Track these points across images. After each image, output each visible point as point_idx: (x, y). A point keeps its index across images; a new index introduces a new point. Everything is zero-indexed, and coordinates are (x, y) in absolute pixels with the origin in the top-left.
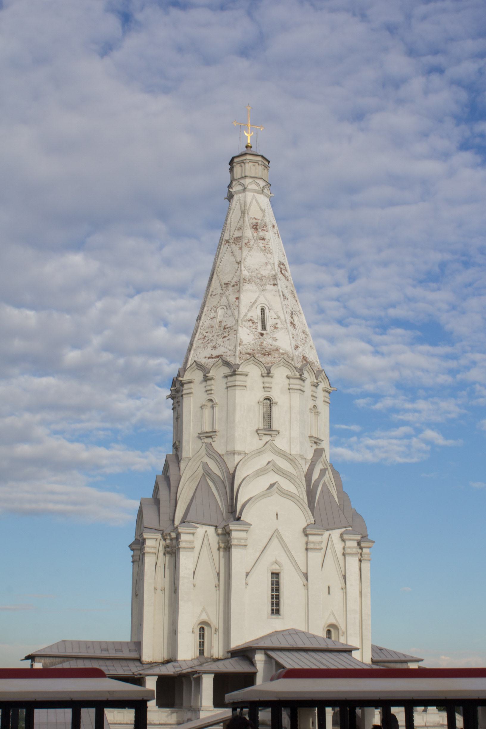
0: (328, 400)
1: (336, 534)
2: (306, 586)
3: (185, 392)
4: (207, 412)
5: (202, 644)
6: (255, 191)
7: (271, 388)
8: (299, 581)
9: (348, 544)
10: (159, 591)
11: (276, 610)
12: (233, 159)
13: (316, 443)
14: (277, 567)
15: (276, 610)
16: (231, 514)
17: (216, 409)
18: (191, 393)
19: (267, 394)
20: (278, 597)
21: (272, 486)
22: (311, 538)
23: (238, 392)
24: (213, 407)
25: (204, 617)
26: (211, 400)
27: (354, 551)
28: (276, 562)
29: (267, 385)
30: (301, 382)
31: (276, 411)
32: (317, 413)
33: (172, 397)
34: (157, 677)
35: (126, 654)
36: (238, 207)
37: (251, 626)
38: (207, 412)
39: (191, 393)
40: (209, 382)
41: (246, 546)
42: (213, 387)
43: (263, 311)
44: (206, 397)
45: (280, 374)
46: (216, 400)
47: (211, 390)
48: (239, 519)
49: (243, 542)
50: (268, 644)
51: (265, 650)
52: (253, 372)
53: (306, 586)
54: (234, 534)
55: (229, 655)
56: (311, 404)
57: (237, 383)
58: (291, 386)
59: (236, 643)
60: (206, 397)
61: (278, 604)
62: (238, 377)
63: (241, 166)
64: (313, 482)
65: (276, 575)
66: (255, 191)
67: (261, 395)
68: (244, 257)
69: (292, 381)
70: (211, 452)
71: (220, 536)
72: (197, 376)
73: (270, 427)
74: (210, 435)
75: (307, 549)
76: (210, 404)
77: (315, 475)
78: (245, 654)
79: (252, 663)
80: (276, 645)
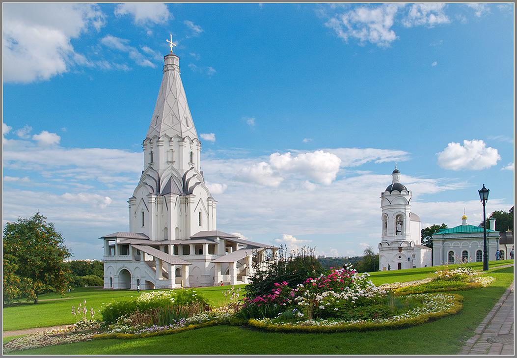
16: (187, 191)
17: (174, 153)
23: (184, 148)
28: (200, 209)
36: (171, 76)
37: (195, 230)
38: (170, 154)
40: (171, 143)
44: (169, 149)
46: (174, 150)
53: (208, 218)
54: (191, 199)
60: (169, 149)
62: (184, 143)
70: (173, 169)
74: (172, 162)
75: (208, 205)
76: (171, 151)
80: (221, 236)
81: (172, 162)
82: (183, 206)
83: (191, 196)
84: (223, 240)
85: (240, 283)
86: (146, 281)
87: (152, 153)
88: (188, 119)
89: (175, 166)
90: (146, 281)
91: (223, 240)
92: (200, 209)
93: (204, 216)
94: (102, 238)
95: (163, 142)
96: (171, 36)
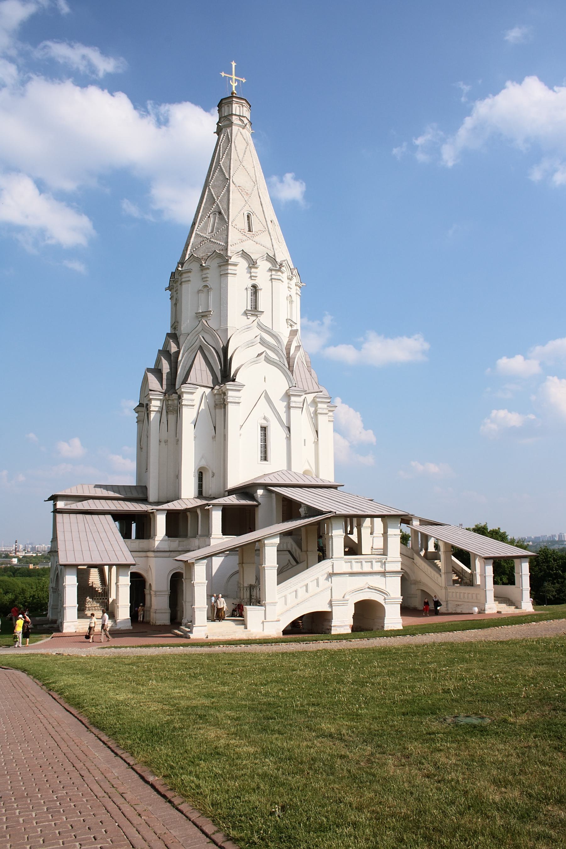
0: (299, 293)
1: (310, 398)
2: (289, 439)
3: (183, 280)
4: (202, 296)
5: (200, 486)
6: (240, 126)
7: (256, 277)
8: (283, 433)
9: (320, 405)
10: (163, 444)
11: (265, 458)
12: (222, 100)
13: (291, 325)
14: (265, 422)
15: (265, 458)
17: (211, 294)
18: (189, 281)
19: (253, 282)
20: (265, 446)
21: (259, 355)
22: (293, 399)
24: (208, 291)
25: (203, 463)
26: (206, 286)
27: (326, 411)
28: (265, 418)
29: (253, 274)
30: (279, 273)
31: (260, 294)
32: (291, 302)
33: (170, 288)
34: (166, 512)
35: (135, 495)
39: (189, 281)
40: (205, 272)
41: (239, 403)
42: (208, 275)
43: (248, 217)
45: (264, 266)
47: (207, 277)
48: (234, 380)
49: (237, 400)
50: (267, 481)
51: (265, 486)
52: (243, 264)
53: (289, 439)
54: (230, 393)
55: (227, 493)
56: (287, 293)
57: (229, 271)
58: (273, 277)
59: (233, 482)
61: (265, 452)
62: (230, 267)
63: (228, 106)
64: (291, 354)
65: (264, 429)
66: (240, 126)
67: (250, 283)
68: (231, 175)
69: (274, 273)
70: (205, 330)
71: (217, 397)
72: (195, 267)
73: (256, 308)
74: (205, 315)
75: (289, 407)
76: (205, 290)
77: (292, 352)
78: (246, 491)
79: (253, 498)
80: (275, 481)
81: (205, 315)
82: (219, 412)
83: (229, 385)
84: (274, 495)
85: (227, 630)
86: (279, 583)
87: (176, 304)
88: (253, 218)
89: (212, 323)
90: (279, 583)
91: (274, 495)
92: (265, 418)
93: (276, 435)
94: (50, 499)
95: (189, 274)
96: (234, 64)
